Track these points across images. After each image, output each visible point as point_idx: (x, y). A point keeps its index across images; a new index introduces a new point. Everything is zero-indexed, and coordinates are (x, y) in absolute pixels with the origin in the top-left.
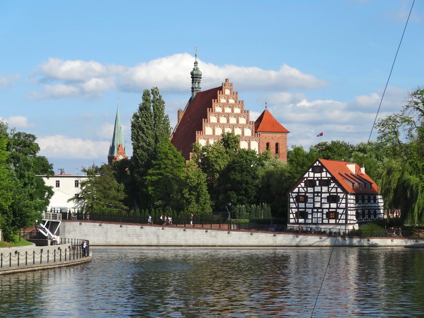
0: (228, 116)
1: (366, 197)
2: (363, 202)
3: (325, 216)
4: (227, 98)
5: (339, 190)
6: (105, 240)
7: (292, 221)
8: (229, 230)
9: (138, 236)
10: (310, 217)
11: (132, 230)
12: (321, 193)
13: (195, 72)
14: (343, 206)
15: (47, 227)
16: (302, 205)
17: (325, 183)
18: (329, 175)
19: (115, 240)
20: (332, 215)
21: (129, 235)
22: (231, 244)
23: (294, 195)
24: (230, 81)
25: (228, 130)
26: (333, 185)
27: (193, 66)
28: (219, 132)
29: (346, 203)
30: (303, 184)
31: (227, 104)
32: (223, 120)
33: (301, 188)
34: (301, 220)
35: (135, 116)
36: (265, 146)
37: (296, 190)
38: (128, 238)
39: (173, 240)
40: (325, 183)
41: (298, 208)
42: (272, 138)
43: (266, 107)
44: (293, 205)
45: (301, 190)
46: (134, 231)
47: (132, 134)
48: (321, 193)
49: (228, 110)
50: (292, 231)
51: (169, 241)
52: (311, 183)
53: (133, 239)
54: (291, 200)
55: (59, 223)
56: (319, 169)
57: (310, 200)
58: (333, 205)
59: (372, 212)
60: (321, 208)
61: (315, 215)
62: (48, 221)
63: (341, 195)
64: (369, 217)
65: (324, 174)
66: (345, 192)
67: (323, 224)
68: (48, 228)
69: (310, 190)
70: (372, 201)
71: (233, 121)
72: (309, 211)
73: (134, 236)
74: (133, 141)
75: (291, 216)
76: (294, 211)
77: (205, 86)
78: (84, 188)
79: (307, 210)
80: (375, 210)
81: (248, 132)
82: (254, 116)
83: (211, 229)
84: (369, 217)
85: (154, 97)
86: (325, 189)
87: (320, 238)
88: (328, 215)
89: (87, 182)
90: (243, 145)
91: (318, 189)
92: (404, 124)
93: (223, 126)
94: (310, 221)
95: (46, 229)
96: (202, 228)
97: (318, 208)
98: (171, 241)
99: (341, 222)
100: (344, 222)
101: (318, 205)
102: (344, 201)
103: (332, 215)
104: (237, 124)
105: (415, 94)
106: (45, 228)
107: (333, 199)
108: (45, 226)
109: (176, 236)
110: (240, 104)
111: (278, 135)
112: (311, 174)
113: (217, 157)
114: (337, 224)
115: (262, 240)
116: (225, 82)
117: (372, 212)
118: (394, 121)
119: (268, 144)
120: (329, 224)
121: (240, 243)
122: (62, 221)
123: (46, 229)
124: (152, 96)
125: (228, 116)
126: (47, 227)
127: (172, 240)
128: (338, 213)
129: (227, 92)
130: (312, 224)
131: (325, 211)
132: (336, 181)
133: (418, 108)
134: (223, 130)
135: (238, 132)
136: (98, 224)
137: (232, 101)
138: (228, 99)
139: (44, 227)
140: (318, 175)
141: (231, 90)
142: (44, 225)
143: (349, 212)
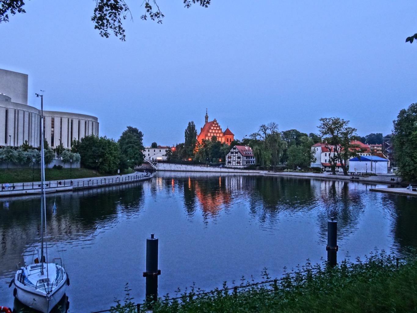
0: (215, 130)
1: (250, 157)
2: (249, 159)
3: (236, 163)
5: (241, 155)
7: (226, 164)
8: (207, 167)
9: (180, 168)
10: (232, 163)
12: (235, 156)
13: (207, 116)
14: (242, 160)
16: (230, 159)
17: (236, 153)
18: (238, 151)
20: (239, 163)
21: (177, 168)
23: (227, 156)
25: (215, 135)
26: (239, 153)
27: (205, 115)
28: (212, 135)
29: (243, 159)
30: (230, 153)
31: (215, 126)
32: (214, 131)
33: (229, 154)
34: (229, 164)
35: (186, 130)
36: (227, 139)
37: (228, 155)
40: (236, 153)
41: (228, 160)
42: (229, 137)
44: (227, 159)
45: (230, 155)
48: (235, 156)
49: (215, 128)
50: (226, 168)
52: (232, 153)
54: (227, 158)
56: (235, 149)
57: (232, 158)
58: (239, 160)
59: (252, 162)
60: (235, 160)
61: (233, 162)
63: (241, 157)
64: (251, 163)
65: (236, 150)
66: (242, 156)
67: (236, 165)
69: (232, 155)
70: (252, 158)
71: (217, 131)
72: (232, 161)
75: (226, 163)
76: (227, 161)
77: (210, 120)
79: (231, 161)
80: (254, 161)
81: (221, 135)
82: (223, 131)
83: (202, 166)
84: (251, 163)
86: (237, 155)
87: (26, 192)
88: (237, 162)
89: (168, 151)
90: (220, 139)
91: (234, 155)
92: (258, 136)
93: (214, 133)
94: (232, 164)
96: (199, 166)
97: (234, 160)
99: (241, 165)
100: (242, 165)
101: (234, 159)
102: (242, 158)
103: (239, 163)
104: (218, 133)
105: (262, 127)
107: (239, 158)
109: (191, 168)
110: (219, 127)
111: (231, 136)
112: (233, 150)
113: (209, 143)
114: (240, 165)
117: (252, 162)
118: (255, 135)
119: (228, 139)
120: (237, 165)
124: (191, 124)
125: (215, 130)
128: (240, 162)
129: (215, 123)
130: (232, 165)
131: (236, 161)
132: (240, 153)
133: (263, 131)
134: (214, 135)
135: (218, 135)
136: (168, 164)
137: (216, 126)
140: (234, 150)
143: (244, 162)
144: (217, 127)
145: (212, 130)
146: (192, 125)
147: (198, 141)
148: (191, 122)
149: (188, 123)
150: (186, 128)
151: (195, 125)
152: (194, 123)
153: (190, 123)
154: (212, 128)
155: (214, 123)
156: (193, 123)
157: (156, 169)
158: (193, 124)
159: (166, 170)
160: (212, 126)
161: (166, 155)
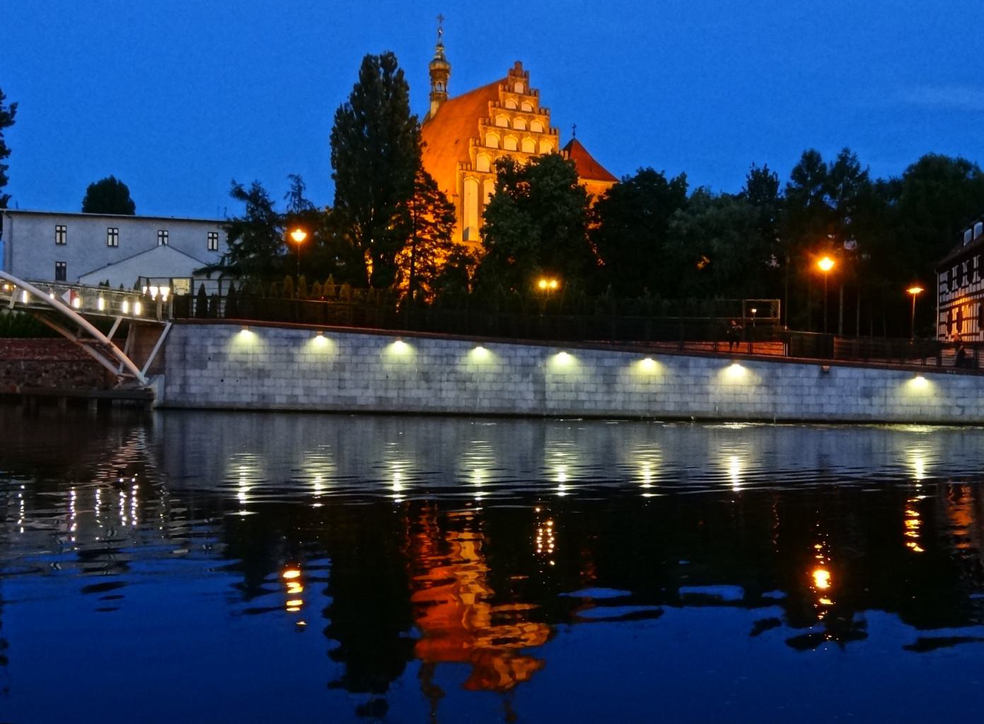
4: (521, 98)
6: (336, 392)
11: (441, 357)
13: (439, 65)
15: (120, 338)
19: (370, 393)
22: (831, 414)
24: (525, 68)
38: (423, 384)
39: (599, 397)
43: (574, 134)
46: (445, 359)
47: (332, 154)
49: (520, 124)
51: (583, 401)
53: (441, 390)
55: (162, 327)
62: (123, 322)
68: (122, 350)
73: (448, 381)
74: (334, 168)
78: (238, 242)
85: (386, 74)
95: (116, 349)
98: (590, 401)
106: (112, 344)
108: (114, 339)
115: (960, 402)
116: (514, 68)
121: (868, 412)
122: (174, 322)
123: (116, 349)
126: (120, 338)
127: (592, 397)
129: (519, 87)
138: (520, 103)
139: (106, 340)
141: (526, 83)
142: (106, 335)
144: (530, 116)
145: (503, 132)
146: (387, 83)
147: (441, 188)
148: (377, 51)
149: (360, 63)
150: (342, 96)
151: (405, 78)
152: (401, 64)
153: (369, 64)
154: (502, 120)
155: (511, 90)
156: (388, 62)
157: (148, 395)
158: (394, 74)
159: (280, 400)
160: (502, 107)
161: (227, 271)
